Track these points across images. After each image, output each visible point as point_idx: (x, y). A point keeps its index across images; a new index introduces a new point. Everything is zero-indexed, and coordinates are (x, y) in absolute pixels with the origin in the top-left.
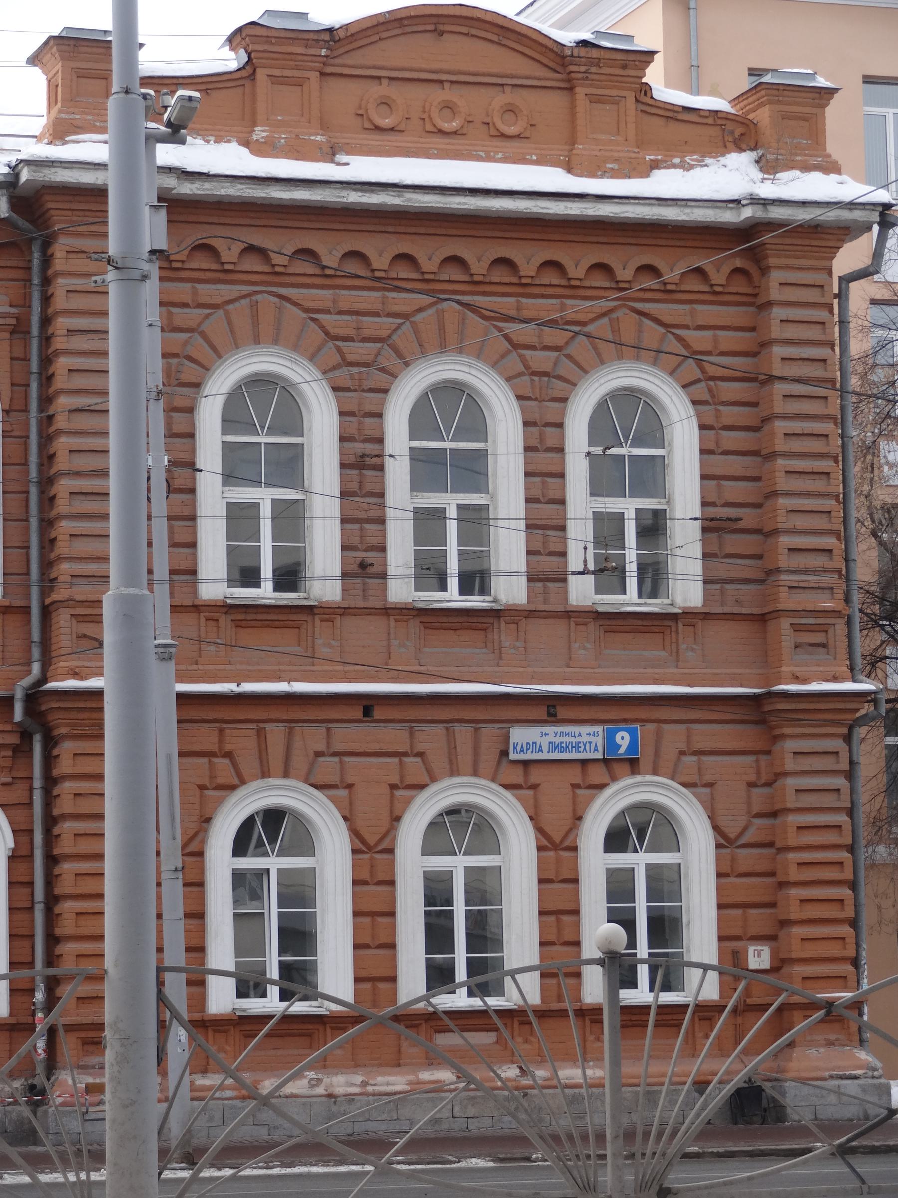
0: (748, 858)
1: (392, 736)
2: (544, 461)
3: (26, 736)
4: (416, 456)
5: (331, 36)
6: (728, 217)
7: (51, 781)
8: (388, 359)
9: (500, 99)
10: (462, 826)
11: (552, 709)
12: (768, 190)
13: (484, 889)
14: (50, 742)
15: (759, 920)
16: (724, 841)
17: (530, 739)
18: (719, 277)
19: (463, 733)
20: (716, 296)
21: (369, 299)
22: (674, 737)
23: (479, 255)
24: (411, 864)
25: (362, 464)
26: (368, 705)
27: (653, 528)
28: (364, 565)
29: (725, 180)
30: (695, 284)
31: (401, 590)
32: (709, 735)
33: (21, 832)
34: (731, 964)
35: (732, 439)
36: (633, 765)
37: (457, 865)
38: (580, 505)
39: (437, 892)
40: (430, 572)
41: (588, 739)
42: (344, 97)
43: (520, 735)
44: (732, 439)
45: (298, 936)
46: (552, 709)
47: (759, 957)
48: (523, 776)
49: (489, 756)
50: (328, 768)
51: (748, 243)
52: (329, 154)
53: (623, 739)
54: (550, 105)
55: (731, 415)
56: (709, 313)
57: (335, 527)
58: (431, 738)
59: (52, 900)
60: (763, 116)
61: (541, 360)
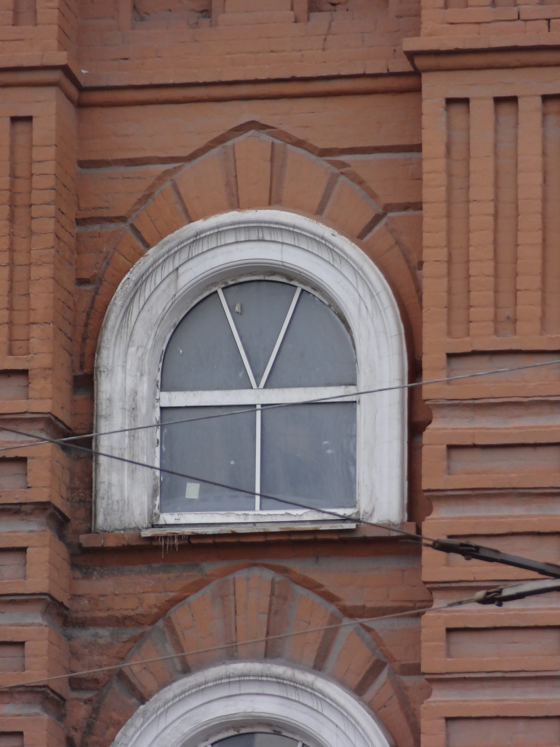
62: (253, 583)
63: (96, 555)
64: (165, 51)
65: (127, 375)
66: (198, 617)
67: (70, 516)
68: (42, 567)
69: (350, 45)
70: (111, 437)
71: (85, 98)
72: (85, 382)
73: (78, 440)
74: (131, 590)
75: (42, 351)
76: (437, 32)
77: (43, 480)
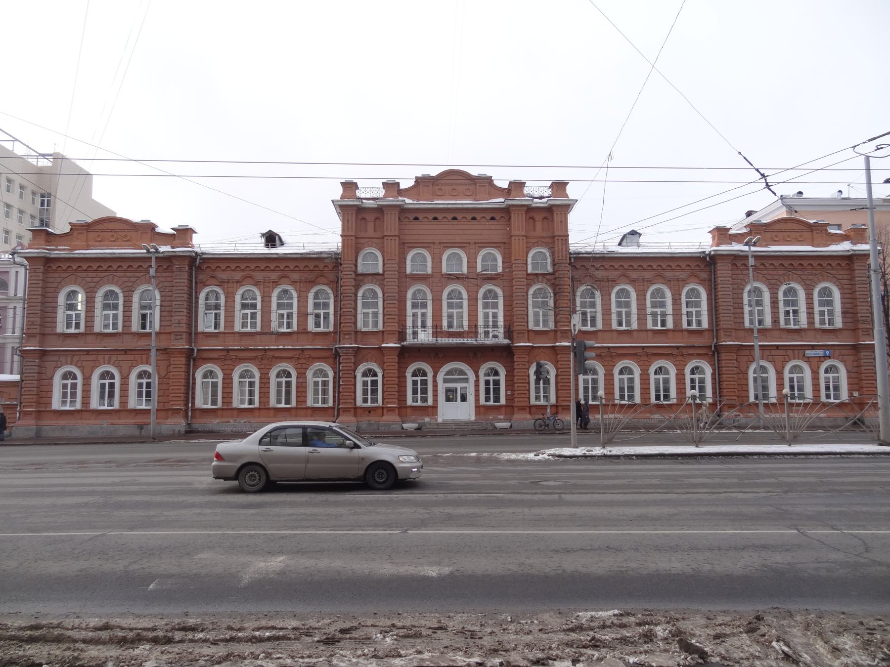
0: (853, 375)
1: (782, 352)
2: (809, 301)
3: (714, 352)
4: (785, 301)
5: (766, 225)
6: (846, 254)
7: (718, 361)
8: (778, 283)
9: (799, 234)
10: (796, 369)
11: (813, 347)
12: (855, 248)
13: (801, 380)
14: (718, 354)
15: (856, 387)
16: (848, 372)
17: (809, 353)
18: (843, 265)
19: (796, 352)
20: (842, 269)
21: (774, 272)
22: (837, 352)
23: (796, 263)
24: (787, 375)
25: (774, 303)
26: (777, 346)
27: (831, 313)
28: (776, 321)
29: (845, 247)
30: (791, 267)
31: (817, 326)
32: (844, 352)
33: (714, 370)
34: (851, 395)
35: (846, 296)
36: (829, 357)
37: (795, 376)
38: (817, 309)
39: (791, 380)
40: (822, 322)
41: (821, 353)
42: (769, 235)
43: (807, 352)
44: (846, 296)
45: (765, 388)
46: (813, 347)
47: (856, 394)
48: (808, 360)
49: (801, 355)
50: (771, 358)
51: (850, 259)
52: (766, 246)
53: (828, 353)
54: (808, 234)
55: (846, 291)
56: (841, 272)
57: (805, 314)
58: (790, 353)
59: (720, 382)
60: (852, 233)
61: (808, 282)
62: (370, 277)
63: (357, 275)
64: (362, 235)
65: (360, 260)
66: (366, 280)
67: (356, 272)
68: (353, 276)
69: (378, 235)
70: (359, 265)
71: (356, 238)
72: (356, 261)
73: (356, 266)
74: (360, 278)
75: (354, 259)
76: (386, 233)
77: (354, 269)
